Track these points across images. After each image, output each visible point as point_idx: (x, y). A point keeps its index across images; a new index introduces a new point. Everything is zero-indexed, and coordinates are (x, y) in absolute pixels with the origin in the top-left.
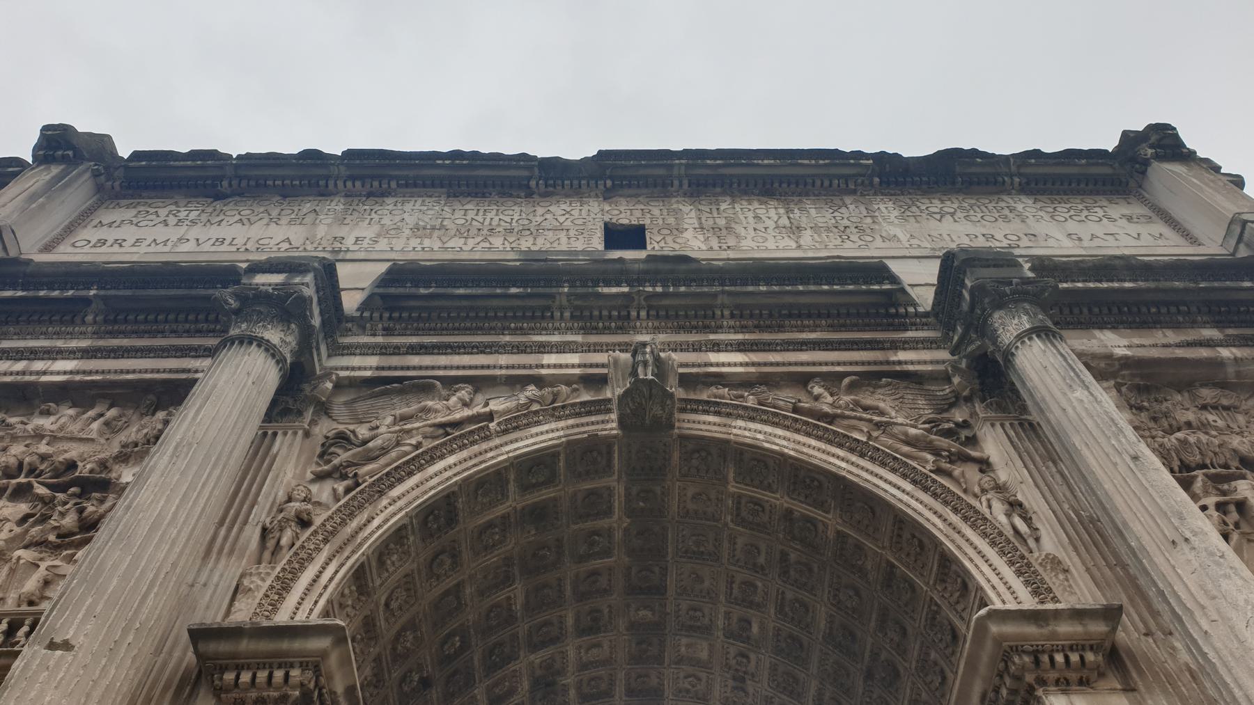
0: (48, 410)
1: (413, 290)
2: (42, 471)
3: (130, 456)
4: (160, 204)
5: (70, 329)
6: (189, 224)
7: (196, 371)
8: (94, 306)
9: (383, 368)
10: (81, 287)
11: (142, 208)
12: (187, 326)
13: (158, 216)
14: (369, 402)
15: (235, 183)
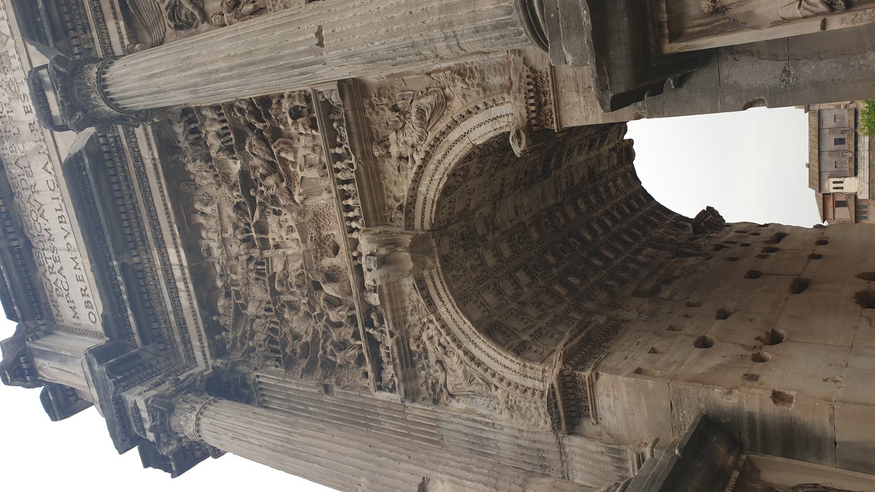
0: (206, 250)
1: (42, 13)
2: (245, 224)
3: (223, 173)
4: (48, 285)
5: (148, 270)
6: (56, 252)
7: (154, 159)
8: (126, 261)
9: (115, 13)
10: (113, 273)
11: (55, 296)
12: (124, 188)
13: (57, 280)
14: (144, 15)
15: (11, 236)
